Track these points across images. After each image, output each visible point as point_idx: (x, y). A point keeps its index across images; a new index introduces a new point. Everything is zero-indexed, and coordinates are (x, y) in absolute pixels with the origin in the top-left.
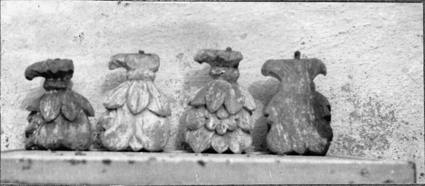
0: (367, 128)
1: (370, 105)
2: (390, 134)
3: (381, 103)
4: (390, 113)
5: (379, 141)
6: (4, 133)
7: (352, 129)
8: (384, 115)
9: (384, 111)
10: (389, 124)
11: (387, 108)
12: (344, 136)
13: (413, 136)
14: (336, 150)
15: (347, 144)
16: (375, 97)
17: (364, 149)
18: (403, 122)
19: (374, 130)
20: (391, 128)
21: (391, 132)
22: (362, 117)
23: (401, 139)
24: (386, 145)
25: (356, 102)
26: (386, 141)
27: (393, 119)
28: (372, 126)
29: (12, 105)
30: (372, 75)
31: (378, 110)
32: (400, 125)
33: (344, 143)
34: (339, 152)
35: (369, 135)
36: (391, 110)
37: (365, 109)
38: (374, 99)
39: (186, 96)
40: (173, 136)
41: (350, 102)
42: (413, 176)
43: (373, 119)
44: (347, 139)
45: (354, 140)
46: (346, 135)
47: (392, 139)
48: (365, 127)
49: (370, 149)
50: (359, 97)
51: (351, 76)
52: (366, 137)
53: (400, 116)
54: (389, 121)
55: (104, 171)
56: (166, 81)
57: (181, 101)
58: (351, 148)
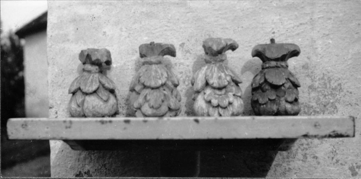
0: (321, 98)
2: (338, 101)
3: (331, 78)
4: (338, 85)
5: (330, 107)
8: (334, 87)
9: (334, 84)
10: (337, 93)
11: (336, 81)
12: (304, 104)
13: (355, 102)
15: (306, 110)
16: (327, 73)
18: (348, 92)
19: (326, 99)
20: (339, 97)
21: (339, 100)
22: (318, 89)
23: (347, 105)
24: (336, 110)
25: (313, 78)
26: (336, 107)
27: (341, 90)
28: (325, 96)
31: (330, 82)
32: (345, 94)
33: (304, 109)
35: (323, 103)
36: (339, 83)
37: (320, 82)
42: (353, 128)
43: (326, 90)
45: (312, 107)
46: (306, 103)
47: (340, 105)
48: (320, 96)
49: (324, 114)
50: (315, 74)
51: (309, 57)
52: (321, 104)
53: (345, 87)
54: (337, 91)
55: (125, 129)
58: (310, 113)
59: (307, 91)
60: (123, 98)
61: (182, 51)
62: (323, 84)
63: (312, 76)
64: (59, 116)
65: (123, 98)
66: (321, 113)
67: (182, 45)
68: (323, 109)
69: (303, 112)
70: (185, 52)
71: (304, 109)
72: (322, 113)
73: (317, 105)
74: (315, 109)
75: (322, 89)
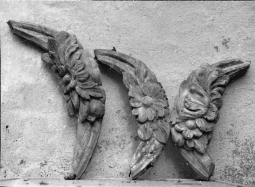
0: (245, 161)
1: (247, 145)
6: (3, 167)
7: (234, 162)
12: (229, 167)
14: (224, 177)
15: (231, 172)
16: (250, 139)
17: (243, 176)
19: (249, 163)
22: (241, 153)
28: (248, 160)
29: (8, 148)
30: (247, 123)
33: (229, 172)
34: (226, 179)
35: (246, 166)
37: (243, 147)
38: (249, 141)
39: (122, 140)
40: (114, 168)
41: (233, 142)
44: (231, 169)
46: (230, 166)
48: (243, 160)
49: (247, 176)
51: (233, 124)
52: (244, 168)
56: (109, 130)
57: (119, 143)
58: (234, 176)
59: (231, 155)
60: (65, 160)
61: (118, 117)
62: (246, 149)
63: (236, 141)
64: (7, 175)
65: (65, 160)
66: (244, 175)
67: (119, 112)
68: (246, 173)
69: (228, 175)
70: (121, 118)
71: (229, 172)
72: (245, 176)
73: (241, 168)
74: (239, 172)
75: (245, 154)
